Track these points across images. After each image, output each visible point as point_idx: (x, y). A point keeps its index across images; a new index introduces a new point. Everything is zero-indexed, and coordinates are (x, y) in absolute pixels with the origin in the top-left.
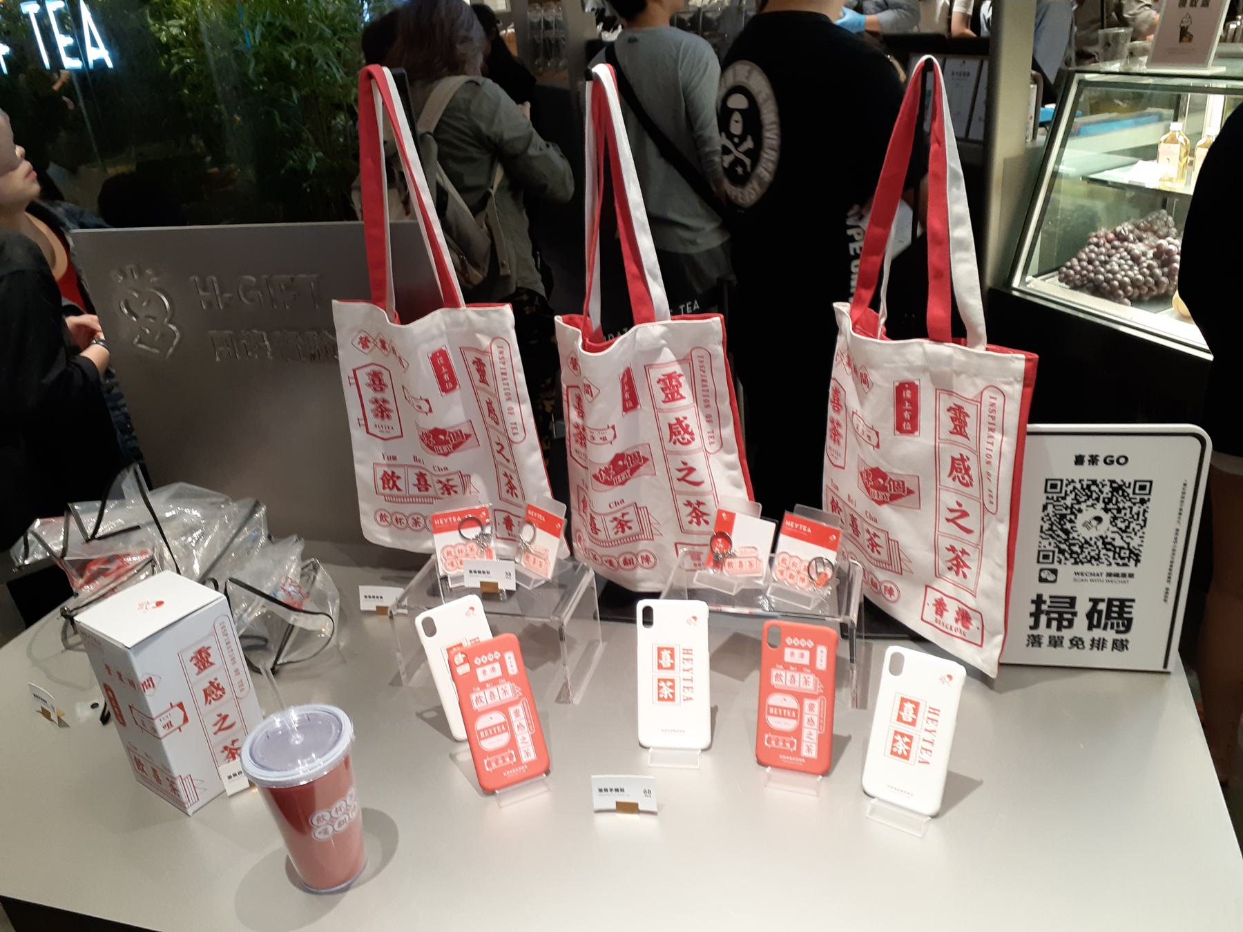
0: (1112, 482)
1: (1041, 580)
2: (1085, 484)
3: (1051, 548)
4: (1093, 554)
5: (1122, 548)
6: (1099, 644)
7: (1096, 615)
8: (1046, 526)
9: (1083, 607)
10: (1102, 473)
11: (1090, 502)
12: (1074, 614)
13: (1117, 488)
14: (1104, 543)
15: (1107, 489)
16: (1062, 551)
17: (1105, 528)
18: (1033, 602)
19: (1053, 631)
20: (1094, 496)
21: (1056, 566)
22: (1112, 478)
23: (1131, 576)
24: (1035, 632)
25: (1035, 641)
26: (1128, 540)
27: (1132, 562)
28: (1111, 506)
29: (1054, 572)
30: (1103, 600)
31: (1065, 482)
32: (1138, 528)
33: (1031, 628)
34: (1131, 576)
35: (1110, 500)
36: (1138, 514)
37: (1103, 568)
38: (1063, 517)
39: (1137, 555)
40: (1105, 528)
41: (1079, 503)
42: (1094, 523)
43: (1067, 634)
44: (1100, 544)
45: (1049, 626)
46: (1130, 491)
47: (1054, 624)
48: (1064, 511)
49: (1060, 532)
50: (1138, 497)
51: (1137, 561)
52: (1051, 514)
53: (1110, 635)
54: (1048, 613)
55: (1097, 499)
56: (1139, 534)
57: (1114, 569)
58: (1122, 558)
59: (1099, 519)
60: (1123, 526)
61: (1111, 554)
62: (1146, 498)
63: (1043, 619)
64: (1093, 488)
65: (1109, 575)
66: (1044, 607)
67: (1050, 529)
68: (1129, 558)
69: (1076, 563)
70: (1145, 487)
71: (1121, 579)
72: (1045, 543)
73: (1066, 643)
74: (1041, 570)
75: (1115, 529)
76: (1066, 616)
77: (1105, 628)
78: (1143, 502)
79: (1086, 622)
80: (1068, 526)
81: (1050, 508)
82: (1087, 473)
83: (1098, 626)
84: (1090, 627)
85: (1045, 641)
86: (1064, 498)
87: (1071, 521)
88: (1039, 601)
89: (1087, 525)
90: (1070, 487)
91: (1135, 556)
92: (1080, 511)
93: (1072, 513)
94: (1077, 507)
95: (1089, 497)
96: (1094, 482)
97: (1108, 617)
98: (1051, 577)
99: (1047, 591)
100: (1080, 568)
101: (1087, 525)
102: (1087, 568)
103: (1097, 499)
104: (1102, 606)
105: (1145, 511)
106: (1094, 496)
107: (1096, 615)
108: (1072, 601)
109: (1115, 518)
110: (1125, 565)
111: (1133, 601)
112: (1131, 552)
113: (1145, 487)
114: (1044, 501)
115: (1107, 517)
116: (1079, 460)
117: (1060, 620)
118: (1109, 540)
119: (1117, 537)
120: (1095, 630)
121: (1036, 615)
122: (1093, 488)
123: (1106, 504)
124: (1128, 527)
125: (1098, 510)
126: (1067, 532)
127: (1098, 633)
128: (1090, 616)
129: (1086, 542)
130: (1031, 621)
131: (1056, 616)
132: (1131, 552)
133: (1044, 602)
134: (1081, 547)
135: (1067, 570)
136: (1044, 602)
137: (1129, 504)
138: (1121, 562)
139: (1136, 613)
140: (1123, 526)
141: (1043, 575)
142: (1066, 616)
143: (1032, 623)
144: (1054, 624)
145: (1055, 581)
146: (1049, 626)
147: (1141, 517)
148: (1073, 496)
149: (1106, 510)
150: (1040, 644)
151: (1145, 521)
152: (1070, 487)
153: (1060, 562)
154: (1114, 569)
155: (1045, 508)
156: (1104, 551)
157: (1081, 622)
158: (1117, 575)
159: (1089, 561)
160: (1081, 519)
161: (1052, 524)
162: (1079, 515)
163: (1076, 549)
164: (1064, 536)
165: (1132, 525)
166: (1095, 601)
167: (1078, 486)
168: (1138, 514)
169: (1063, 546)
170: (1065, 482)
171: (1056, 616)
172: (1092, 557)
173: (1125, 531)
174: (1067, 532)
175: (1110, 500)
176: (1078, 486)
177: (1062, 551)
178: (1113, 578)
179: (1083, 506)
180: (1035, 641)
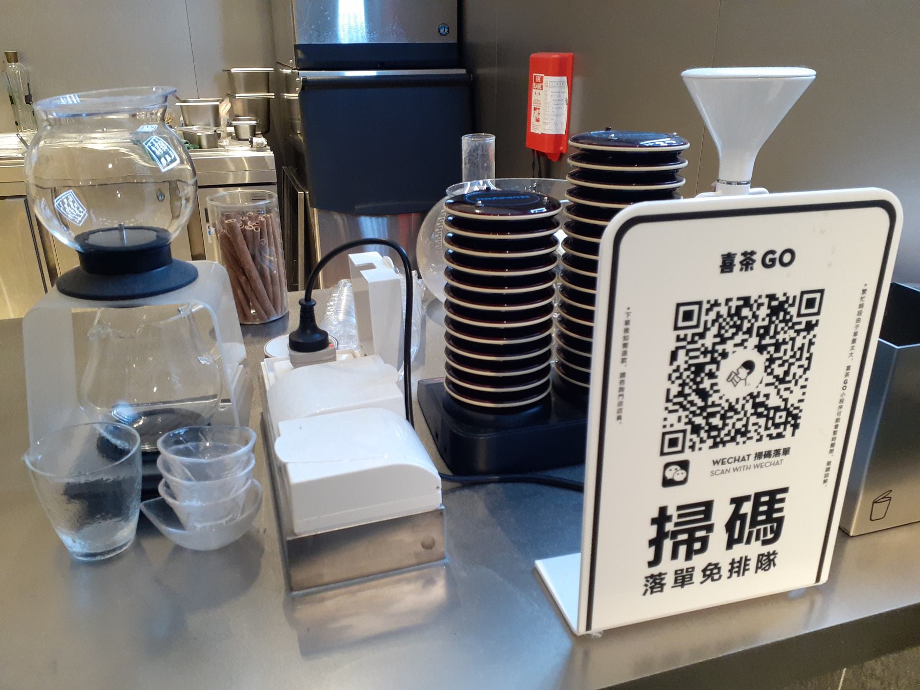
0: (772, 297)
1: (667, 483)
2: (734, 304)
3: (681, 426)
4: (739, 425)
5: (777, 409)
6: (739, 567)
7: (738, 523)
8: (675, 389)
9: (721, 514)
10: (757, 283)
11: (738, 339)
12: (710, 528)
13: (778, 308)
14: (755, 406)
15: (764, 312)
16: (696, 429)
17: (757, 381)
18: (654, 521)
19: (681, 563)
20: (746, 325)
21: (687, 455)
22: (770, 292)
23: (786, 451)
24: (655, 570)
25: (655, 583)
26: (785, 394)
27: (789, 429)
28: (767, 341)
29: (684, 465)
30: (747, 498)
31: (705, 306)
32: (800, 372)
33: (651, 564)
34: (786, 451)
35: (767, 329)
36: (801, 349)
37: (752, 447)
38: (700, 368)
39: (796, 417)
40: (757, 381)
41: (723, 341)
42: (743, 372)
43: (699, 562)
44: (748, 407)
45: (674, 555)
46: (793, 311)
47: (683, 549)
48: (702, 360)
49: (694, 397)
50: (804, 320)
51: (796, 426)
52: (683, 366)
53: (753, 550)
54: (674, 534)
55: (749, 331)
56: (801, 382)
57: (768, 445)
58: (777, 426)
59: (749, 366)
60: (779, 371)
61: (762, 421)
62: (813, 319)
63: (668, 544)
64: (746, 312)
65: (759, 456)
66: (669, 527)
67: (681, 394)
68: (785, 423)
69: (715, 445)
70: (812, 300)
71: (773, 459)
72: (673, 418)
73: (698, 576)
74: (667, 466)
75: (770, 379)
76: (699, 534)
77: (748, 542)
78: (810, 327)
79: (725, 537)
80: (706, 384)
81: (681, 354)
82: (742, 284)
83: (739, 540)
84: (729, 546)
85: (669, 580)
86: (702, 336)
87: (711, 375)
88: (661, 518)
89: (732, 378)
90: (712, 315)
91: (793, 419)
92: (724, 355)
93: (714, 361)
94: (720, 348)
95: (739, 328)
96: (746, 301)
97: (754, 523)
98: (679, 475)
99: (673, 499)
100: (722, 452)
101: (732, 378)
102: (730, 450)
103: (749, 331)
104: (747, 508)
105: (811, 343)
106: (746, 325)
107: (738, 523)
108: (708, 506)
109: (771, 360)
110: (780, 436)
111: (785, 490)
112: (789, 414)
113: (812, 300)
114: (673, 345)
115: (760, 361)
116: (727, 264)
117: (689, 543)
118: (761, 399)
119: (772, 390)
120: (736, 547)
121: (656, 543)
122: (746, 312)
123: (761, 337)
124: (786, 373)
125: (750, 353)
126: (703, 394)
127: (739, 551)
128: (730, 527)
129: (731, 408)
130: (650, 554)
131: (684, 537)
132: (789, 414)
133: (669, 518)
134: (724, 417)
135: (702, 458)
136: (669, 518)
137: (792, 333)
138: (774, 432)
139: (790, 509)
140: (779, 371)
141: (669, 475)
142: (699, 534)
143: (651, 557)
144: (683, 549)
145: (684, 482)
146: (674, 555)
147: (806, 355)
148: (714, 330)
149: (761, 348)
150: (662, 586)
151: (809, 359)
152: (712, 315)
153: (692, 447)
154: (768, 445)
155: (674, 356)
156: (753, 419)
157: (718, 537)
158: (768, 454)
159: (733, 439)
160: (728, 366)
161: (683, 385)
162: (723, 363)
163: (716, 421)
164: (700, 403)
165: (794, 369)
166: (738, 502)
167: (723, 310)
168: (801, 349)
169: (699, 420)
170: (705, 306)
171: (684, 537)
172: (738, 432)
173: (782, 381)
174: (703, 394)
175: (767, 329)
176: (723, 310)
177: (696, 429)
178: (764, 460)
179: (729, 346)
180: (655, 583)
